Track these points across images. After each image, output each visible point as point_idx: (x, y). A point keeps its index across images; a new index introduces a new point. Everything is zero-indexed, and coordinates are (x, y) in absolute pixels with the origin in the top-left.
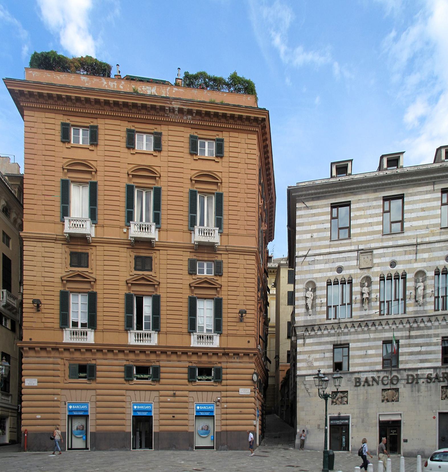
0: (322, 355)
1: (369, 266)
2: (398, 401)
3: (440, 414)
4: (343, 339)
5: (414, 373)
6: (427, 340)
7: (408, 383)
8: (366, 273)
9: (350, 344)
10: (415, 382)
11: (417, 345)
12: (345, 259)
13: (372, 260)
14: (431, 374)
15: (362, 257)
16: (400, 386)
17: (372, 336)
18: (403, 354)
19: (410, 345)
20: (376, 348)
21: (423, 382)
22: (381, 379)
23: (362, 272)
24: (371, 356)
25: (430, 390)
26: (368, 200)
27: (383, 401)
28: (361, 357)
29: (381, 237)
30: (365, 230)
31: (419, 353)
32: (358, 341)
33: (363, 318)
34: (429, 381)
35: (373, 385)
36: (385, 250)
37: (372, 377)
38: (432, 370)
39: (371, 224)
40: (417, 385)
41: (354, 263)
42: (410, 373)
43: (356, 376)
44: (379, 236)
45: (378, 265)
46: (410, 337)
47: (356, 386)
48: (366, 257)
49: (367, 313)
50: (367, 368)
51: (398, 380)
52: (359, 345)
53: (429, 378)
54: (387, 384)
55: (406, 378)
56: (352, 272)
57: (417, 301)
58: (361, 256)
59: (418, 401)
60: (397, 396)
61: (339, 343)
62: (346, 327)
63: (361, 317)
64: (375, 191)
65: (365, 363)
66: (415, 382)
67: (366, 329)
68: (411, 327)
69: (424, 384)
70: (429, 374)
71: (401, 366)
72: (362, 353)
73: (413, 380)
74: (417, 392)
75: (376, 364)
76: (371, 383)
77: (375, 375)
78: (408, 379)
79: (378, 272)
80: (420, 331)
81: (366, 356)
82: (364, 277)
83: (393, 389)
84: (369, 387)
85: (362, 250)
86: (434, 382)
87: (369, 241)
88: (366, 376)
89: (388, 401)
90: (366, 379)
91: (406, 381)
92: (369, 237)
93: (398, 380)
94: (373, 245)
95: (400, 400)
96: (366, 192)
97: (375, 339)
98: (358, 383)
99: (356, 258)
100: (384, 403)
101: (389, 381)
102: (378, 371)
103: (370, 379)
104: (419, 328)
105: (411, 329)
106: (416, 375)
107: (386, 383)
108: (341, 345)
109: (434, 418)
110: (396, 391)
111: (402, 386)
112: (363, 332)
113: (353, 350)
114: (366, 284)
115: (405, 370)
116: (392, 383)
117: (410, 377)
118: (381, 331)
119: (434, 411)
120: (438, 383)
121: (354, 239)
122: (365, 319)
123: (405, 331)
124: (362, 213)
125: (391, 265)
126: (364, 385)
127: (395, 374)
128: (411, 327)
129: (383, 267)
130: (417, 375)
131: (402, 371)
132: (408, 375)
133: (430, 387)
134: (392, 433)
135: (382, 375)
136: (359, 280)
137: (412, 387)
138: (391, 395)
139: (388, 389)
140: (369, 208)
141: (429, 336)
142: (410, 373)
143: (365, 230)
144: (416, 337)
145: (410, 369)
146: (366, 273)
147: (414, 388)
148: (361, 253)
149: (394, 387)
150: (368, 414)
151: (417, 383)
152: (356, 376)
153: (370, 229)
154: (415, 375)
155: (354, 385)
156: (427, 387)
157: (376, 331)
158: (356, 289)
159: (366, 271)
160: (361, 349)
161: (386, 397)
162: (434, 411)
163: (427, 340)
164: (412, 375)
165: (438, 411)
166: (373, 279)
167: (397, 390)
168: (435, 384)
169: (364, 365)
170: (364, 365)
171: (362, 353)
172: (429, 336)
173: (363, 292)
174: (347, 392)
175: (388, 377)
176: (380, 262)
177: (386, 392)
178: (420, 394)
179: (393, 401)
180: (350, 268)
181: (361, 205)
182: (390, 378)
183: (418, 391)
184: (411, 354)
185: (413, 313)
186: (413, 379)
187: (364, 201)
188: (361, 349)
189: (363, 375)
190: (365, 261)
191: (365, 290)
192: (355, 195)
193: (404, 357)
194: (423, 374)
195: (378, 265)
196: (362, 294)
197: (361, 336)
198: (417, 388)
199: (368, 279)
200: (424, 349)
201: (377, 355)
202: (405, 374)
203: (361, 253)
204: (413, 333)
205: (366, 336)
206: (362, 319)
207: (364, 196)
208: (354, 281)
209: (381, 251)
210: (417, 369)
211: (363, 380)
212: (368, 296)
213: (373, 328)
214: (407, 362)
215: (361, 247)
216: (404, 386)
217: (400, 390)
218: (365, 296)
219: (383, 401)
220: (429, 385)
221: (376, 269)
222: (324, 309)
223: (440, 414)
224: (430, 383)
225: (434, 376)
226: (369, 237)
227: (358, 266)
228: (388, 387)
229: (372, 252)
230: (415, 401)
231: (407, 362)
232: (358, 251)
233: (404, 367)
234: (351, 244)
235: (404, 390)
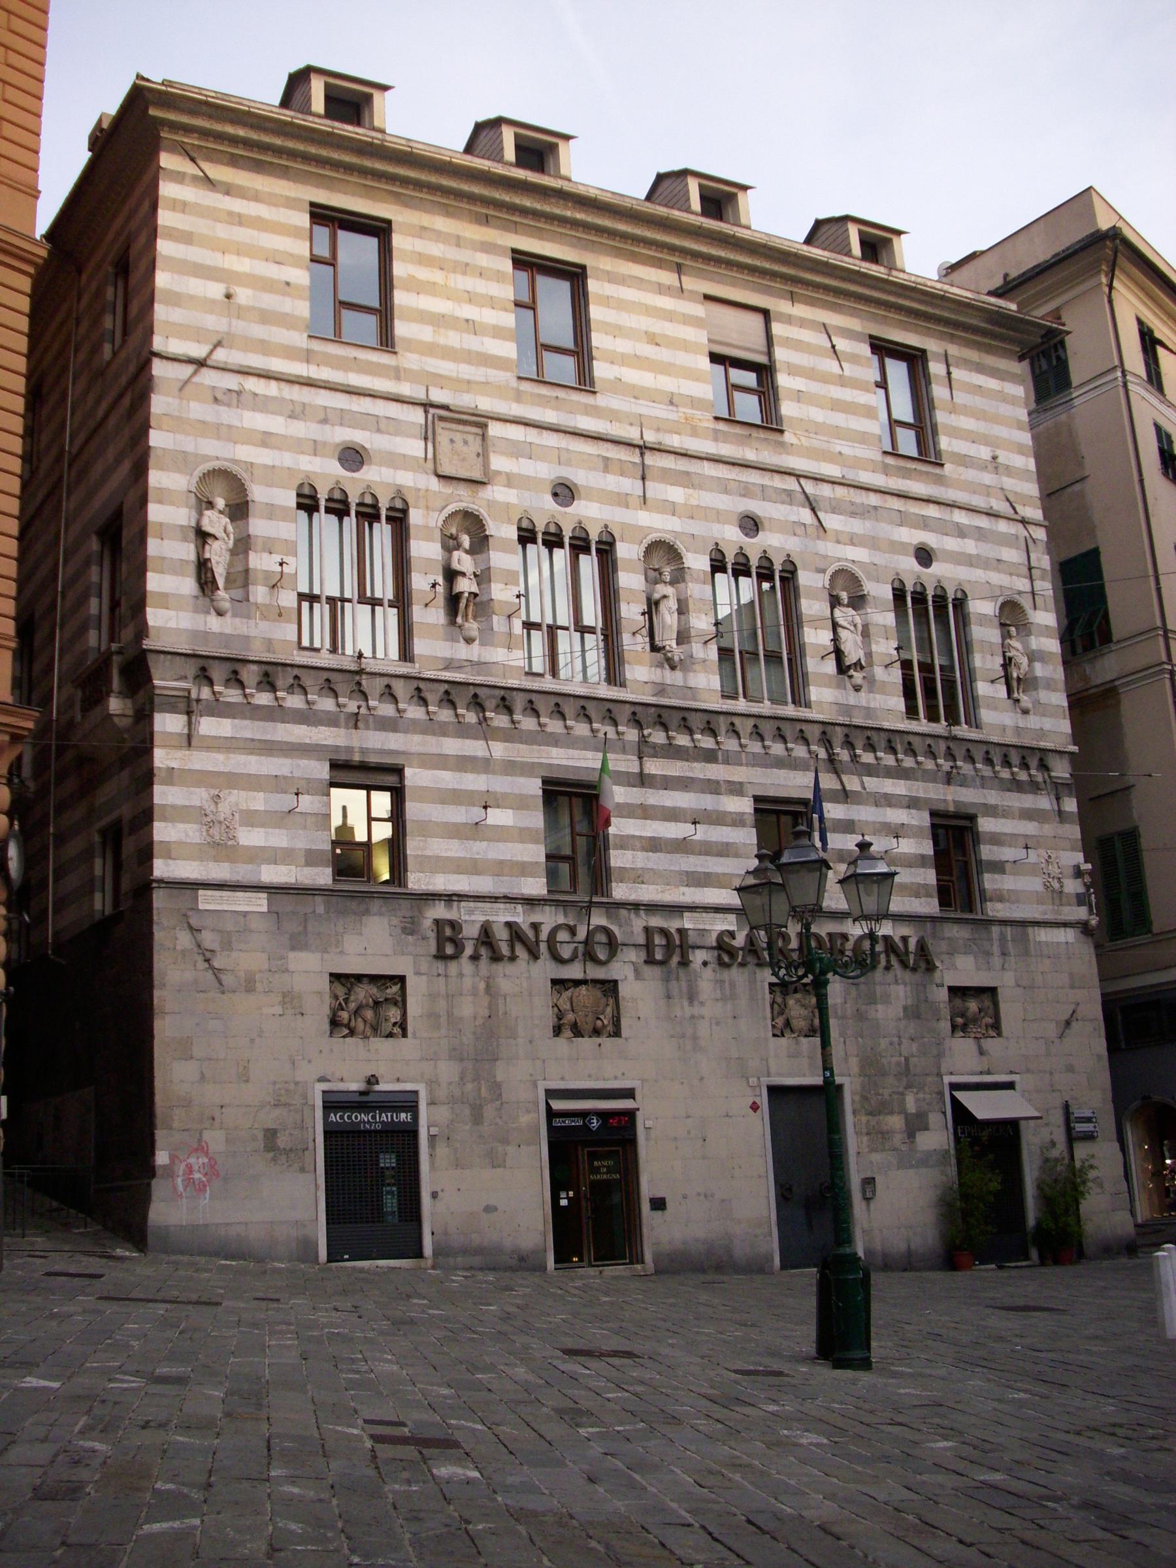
0: (288, 800)
1: (476, 475)
2: (617, 1033)
3: (774, 1091)
4: (375, 743)
5: (673, 925)
6: (707, 802)
7: (650, 961)
8: (463, 498)
9: (408, 772)
10: (675, 959)
11: (672, 815)
12: (377, 424)
13: (484, 455)
14: (732, 934)
15: (444, 435)
16: (622, 969)
17: (499, 750)
18: (626, 843)
19: (645, 812)
20: (519, 803)
21: (705, 964)
22: (544, 936)
23: (448, 489)
24: (501, 834)
25: (733, 997)
26: (458, 241)
27: (557, 1031)
28: (456, 832)
29: (514, 383)
30: (452, 339)
31: (682, 846)
32: (440, 762)
33: (459, 668)
34: (726, 959)
35: (513, 958)
36: (532, 435)
37: (509, 925)
38: (732, 918)
39: (471, 326)
40: (681, 971)
41: (415, 447)
42: (656, 921)
43: (440, 911)
44: (506, 378)
45: (511, 480)
46: (642, 780)
47: (441, 956)
48: (458, 437)
49: (473, 652)
50: (484, 884)
51: (613, 945)
52: (448, 779)
53: (723, 947)
54: (572, 960)
55: (641, 940)
56: (406, 479)
57: (654, 648)
58: (439, 430)
59: (695, 1038)
60: (609, 1010)
61: (357, 758)
62: (389, 694)
63: (449, 665)
64: (486, 221)
65: (474, 862)
66: (675, 959)
67: (471, 717)
68: (643, 740)
69: (709, 969)
70: (722, 933)
71: (620, 891)
72: (459, 815)
73: (669, 951)
74: (686, 1003)
75: (523, 869)
76: (505, 950)
77: (519, 916)
78: (649, 947)
79: (508, 506)
80: (679, 764)
81: (476, 830)
82: (453, 515)
83: (596, 982)
84: (500, 968)
85: (445, 407)
86: (743, 965)
87: (468, 385)
88: (481, 918)
89: (577, 1032)
90: (486, 931)
91: (643, 955)
92: (466, 371)
93: (613, 945)
94: (485, 404)
95: (625, 1032)
96: (447, 212)
97: (511, 768)
98: (448, 942)
99: (420, 432)
100: (561, 1042)
101: (581, 948)
102: (530, 902)
103: (502, 934)
104: (671, 752)
105: (643, 749)
106: (680, 931)
107: (566, 952)
108: (364, 767)
109: (755, 1107)
110: (605, 994)
111: (629, 972)
112: (461, 730)
113: (421, 800)
114: (466, 540)
115: (636, 906)
116: (590, 956)
117: (658, 940)
118: (530, 739)
119: (753, 1081)
120: (758, 970)
121: (409, 360)
122: (472, 679)
123: (624, 751)
124: (437, 276)
125: (555, 495)
126: (475, 958)
127: (598, 919)
128: (643, 740)
129: (527, 494)
130: (682, 932)
131: (623, 912)
132: (647, 930)
133: (732, 985)
134: (596, 1170)
135: (549, 918)
136: (436, 520)
137: (666, 980)
138: (589, 1011)
139: (577, 983)
140: (465, 268)
141: (713, 787)
142: (656, 921)
143: (452, 339)
144: (667, 783)
145: (653, 908)
146: (463, 498)
147: (674, 983)
148: (441, 418)
149: (599, 973)
150: (498, 1085)
151: (685, 963)
152: (440, 911)
153: (473, 343)
154: (673, 931)
155: (433, 950)
156: (722, 982)
157: (512, 735)
158: (425, 550)
159: (463, 491)
160: (456, 797)
161: (570, 1017)
162: (753, 1081)
163: (707, 802)
164: (664, 932)
165: (765, 1081)
166: (492, 528)
167: (610, 988)
168: (746, 971)
169: (473, 867)
170: (473, 867)
171: (459, 815)
172: (713, 787)
173: (455, 566)
174: (401, 979)
175: (572, 931)
176: (515, 470)
177: (568, 993)
178: (696, 1010)
179: (597, 1032)
180: (395, 461)
181: (436, 250)
182: (582, 934)
183: (692, 997)
184: (654, 845)
185: (648, 688)
186: (669, 947)
187: (439, 237)
188: (456, 797)
189: (471, 912)
190: (459, 454)
191: (463, 561)
192: (406, 205)
193: (629, 854)
194: (702, 932)
195: (511, 480)
196: (451, 575)
197: (452, 746)
198: (684, 984)
199: (472, 522)
200: (702, 833)
201: (523, 835)
202: (638, 923)
203: (441, 418)
204: (654, 767)
205: (475, 748)
206: (458, 677)
207: (441, 223)
208: (416, 517)
209: (516, 433)
210: (677, 909)
211: (471, 931)
212: (474, 589)
213: (500, 721)
214: (638, 877)
215: (438, 396)
216: (638, 975)
217: (624, 990)
218: (465, 586)
219: (557, 1031)
220: (726, 975)
221: (497, 493)
222: (288, 599)
223: (774, 1091)
224: (728, 966)
225: (740, 941)
226: (466, 371)
227: (430, 465)
228: (574, 972)
229: (484, 426)
230: (683, 1036)
231: (638, 877)
232: (427, 406)
233: (633, 897)
234: (397, 374)
235: (639, 989)
